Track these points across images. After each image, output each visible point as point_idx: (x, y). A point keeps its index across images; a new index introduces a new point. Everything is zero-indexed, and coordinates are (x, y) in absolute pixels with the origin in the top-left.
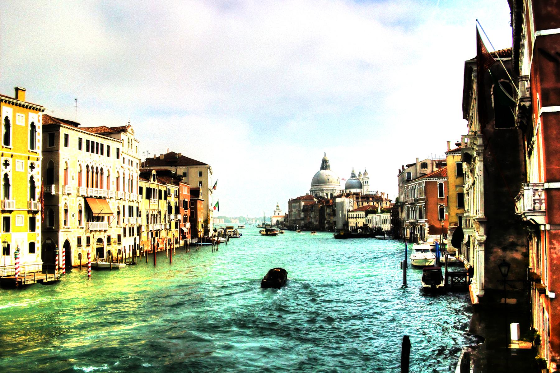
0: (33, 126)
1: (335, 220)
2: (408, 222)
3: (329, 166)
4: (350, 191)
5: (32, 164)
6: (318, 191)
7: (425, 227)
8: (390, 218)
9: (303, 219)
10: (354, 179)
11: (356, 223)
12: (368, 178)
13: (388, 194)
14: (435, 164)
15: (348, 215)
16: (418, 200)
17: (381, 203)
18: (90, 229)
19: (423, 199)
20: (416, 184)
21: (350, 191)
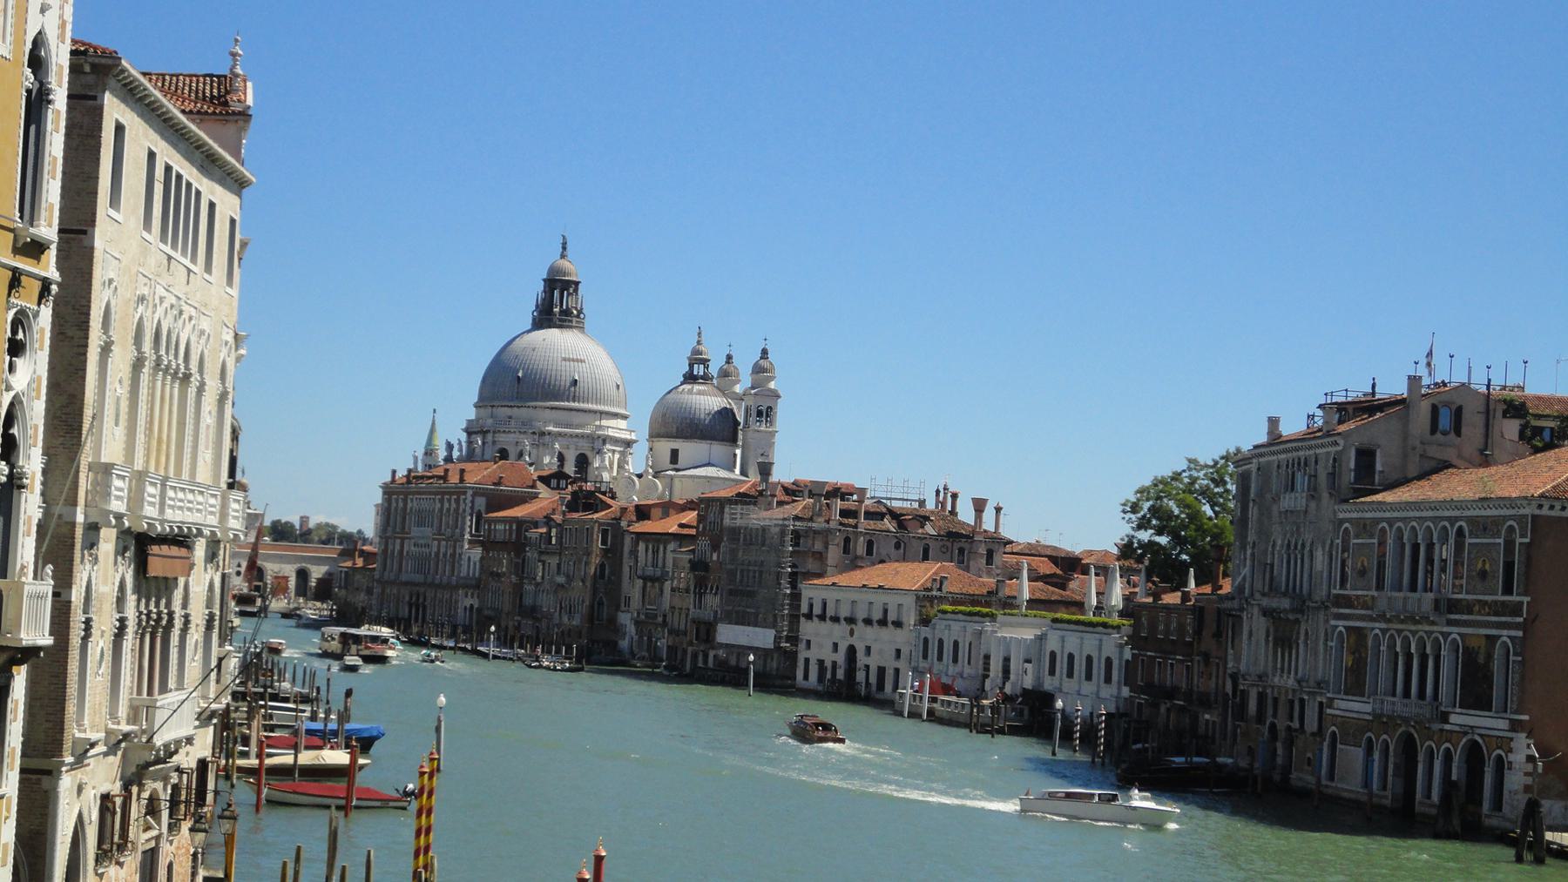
0: (37, 62)
1: (707, 615)
2: (1368, 708)
3: (580, 312)
4: (675, 455)
5: (17, 323)
6: (511, 438)
7: (1511, 757)
8: (1121, 653)
9: (476, 586)
10: (700, 393)
11: (852, 650)
12: (776, 395)
13: (998, 510)
14: (1499, 414)
15: (796, 597)
16: (1454, 606)
17: (961, 551)
18: (159, 741)
19: (1516, 609)
20: (1457, 519)
21: (675, 455)
